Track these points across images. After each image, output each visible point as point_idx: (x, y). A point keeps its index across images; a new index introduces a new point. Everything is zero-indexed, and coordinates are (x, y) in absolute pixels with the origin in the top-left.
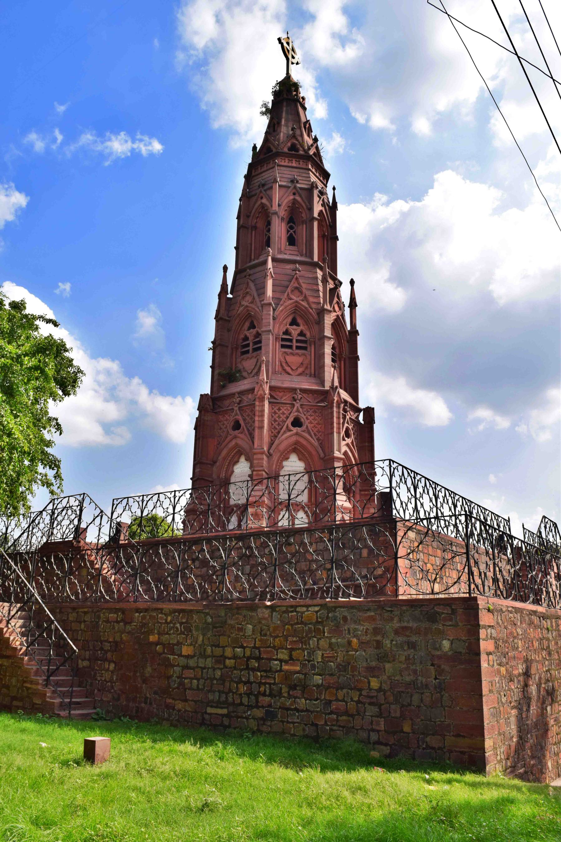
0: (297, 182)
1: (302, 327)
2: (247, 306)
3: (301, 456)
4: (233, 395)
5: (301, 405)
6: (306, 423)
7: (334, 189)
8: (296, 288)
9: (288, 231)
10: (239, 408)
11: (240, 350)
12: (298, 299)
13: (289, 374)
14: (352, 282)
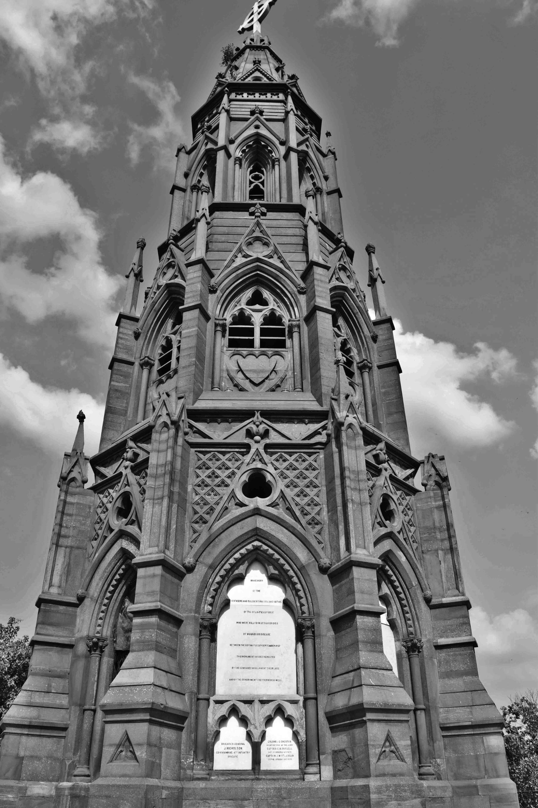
0: (261, 113)
1: (271, 306)
2: (168, 286)
3: (272, 570)
4: (125, 442)
5: (267, 447)
6: (279, 486)
7: (328, 134)
8: (257, 239)
9: (251, 183)
10: (133, 469)
11: (157, 367)
12: (261, 256)
13: (242, 390)
14: (370, 250)
